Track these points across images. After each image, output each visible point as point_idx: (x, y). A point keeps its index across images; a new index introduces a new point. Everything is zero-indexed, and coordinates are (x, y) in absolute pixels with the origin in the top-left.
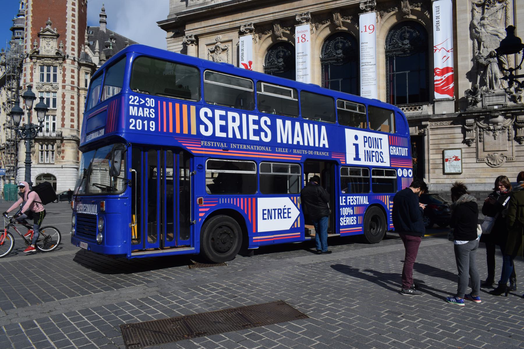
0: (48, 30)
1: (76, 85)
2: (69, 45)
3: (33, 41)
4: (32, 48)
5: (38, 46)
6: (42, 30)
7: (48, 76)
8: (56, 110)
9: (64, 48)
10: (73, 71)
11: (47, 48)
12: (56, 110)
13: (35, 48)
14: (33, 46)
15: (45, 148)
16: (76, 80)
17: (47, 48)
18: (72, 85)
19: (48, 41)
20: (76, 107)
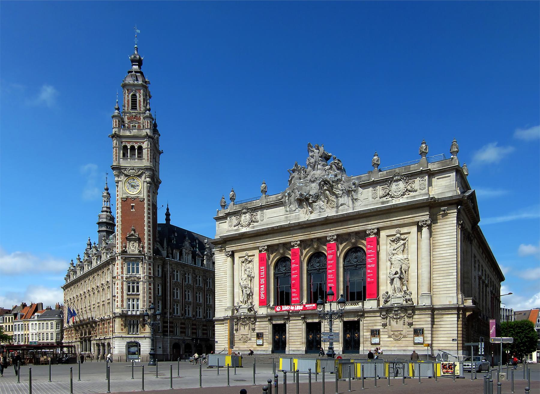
0: (132, 235)
1: (152, 275)
2: (146, 245)
3: (122, 243)
4: (122, 248)
5: (126, 247)
6: (128, 235)
7: (133, 269)
8: (139, 294)
9: (143, 247)
10: (150, 265)
11: (132, 248)
12: (139, 294)
13: (124, 249)
14: (122, 247)
15: (132, 323)
16: (152, 271)
17: (132, 248)
18: (149, 275)
19: (133, 243)
20: (152, 291)
